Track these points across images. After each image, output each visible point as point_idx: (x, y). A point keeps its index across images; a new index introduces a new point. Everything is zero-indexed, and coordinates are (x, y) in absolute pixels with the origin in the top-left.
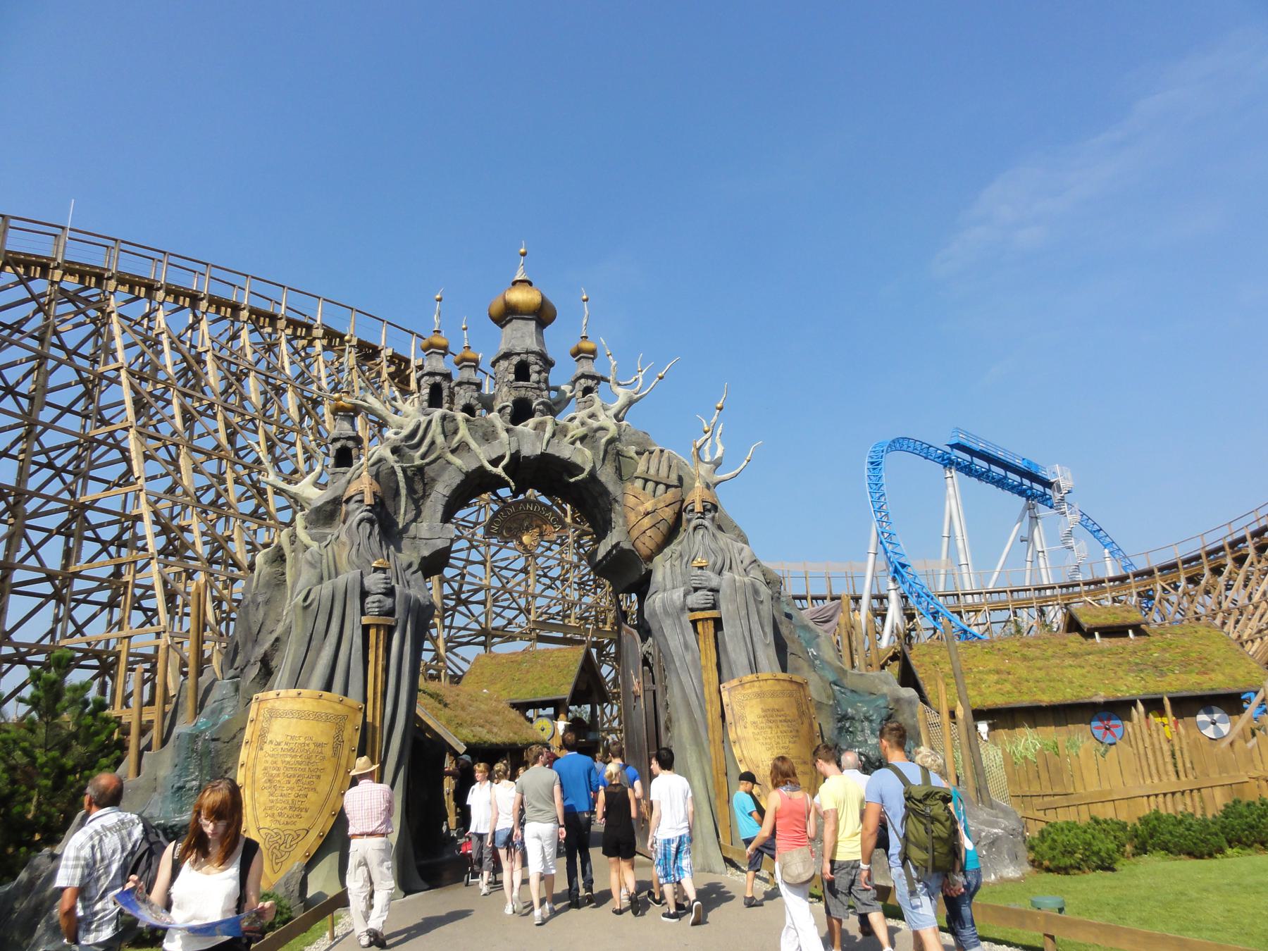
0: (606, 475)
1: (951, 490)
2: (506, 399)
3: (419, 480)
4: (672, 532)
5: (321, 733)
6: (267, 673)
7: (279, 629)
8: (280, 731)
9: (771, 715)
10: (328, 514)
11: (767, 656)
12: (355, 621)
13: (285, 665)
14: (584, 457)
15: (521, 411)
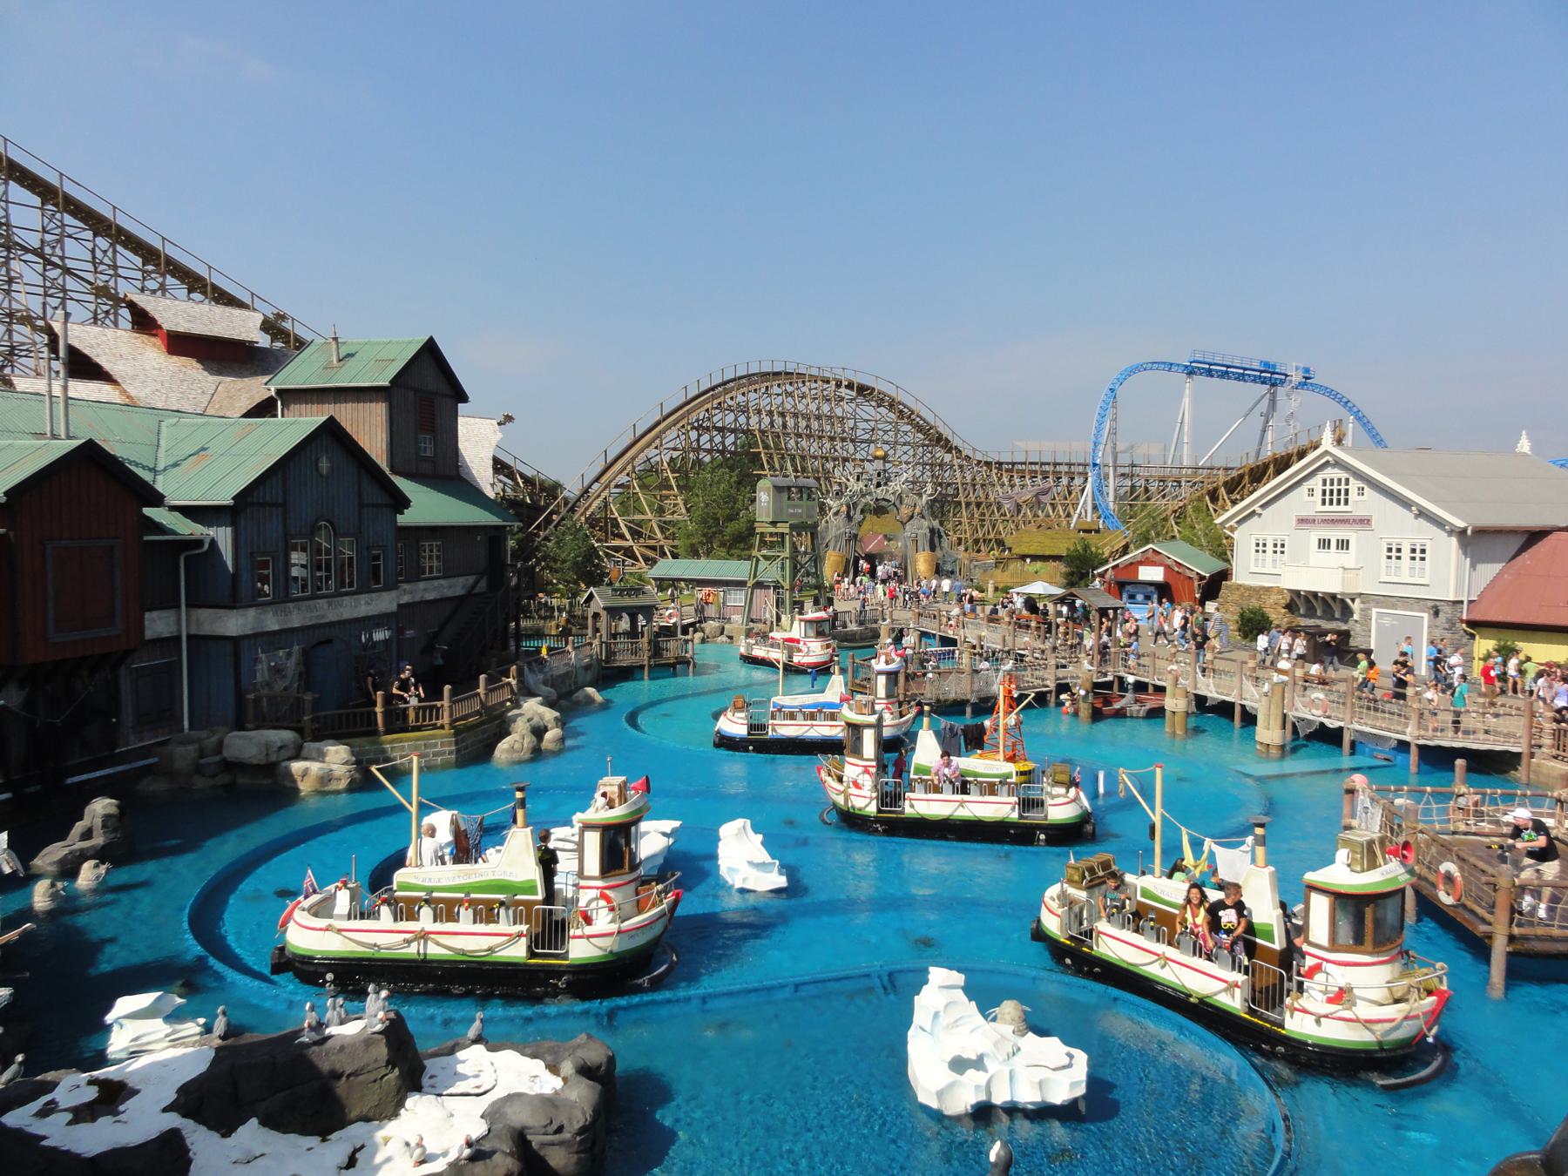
0: (897, 503)
1: (1187, 391)
2: (875, 482)
3: (855, 504)
4: (912, 517)
5: (839, 559)
6: (827, 546)
7: (829, 538)
8: (832, 558)
9: (925, 561)
10: (836, 514)
11: (927, 548)
12: (844, 539)
13: (832, 545)
14: (892, 498)
15: (879, 485)
